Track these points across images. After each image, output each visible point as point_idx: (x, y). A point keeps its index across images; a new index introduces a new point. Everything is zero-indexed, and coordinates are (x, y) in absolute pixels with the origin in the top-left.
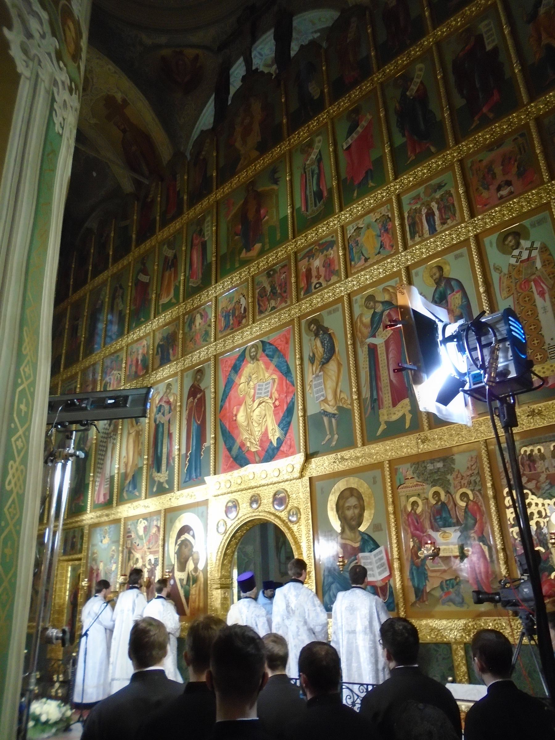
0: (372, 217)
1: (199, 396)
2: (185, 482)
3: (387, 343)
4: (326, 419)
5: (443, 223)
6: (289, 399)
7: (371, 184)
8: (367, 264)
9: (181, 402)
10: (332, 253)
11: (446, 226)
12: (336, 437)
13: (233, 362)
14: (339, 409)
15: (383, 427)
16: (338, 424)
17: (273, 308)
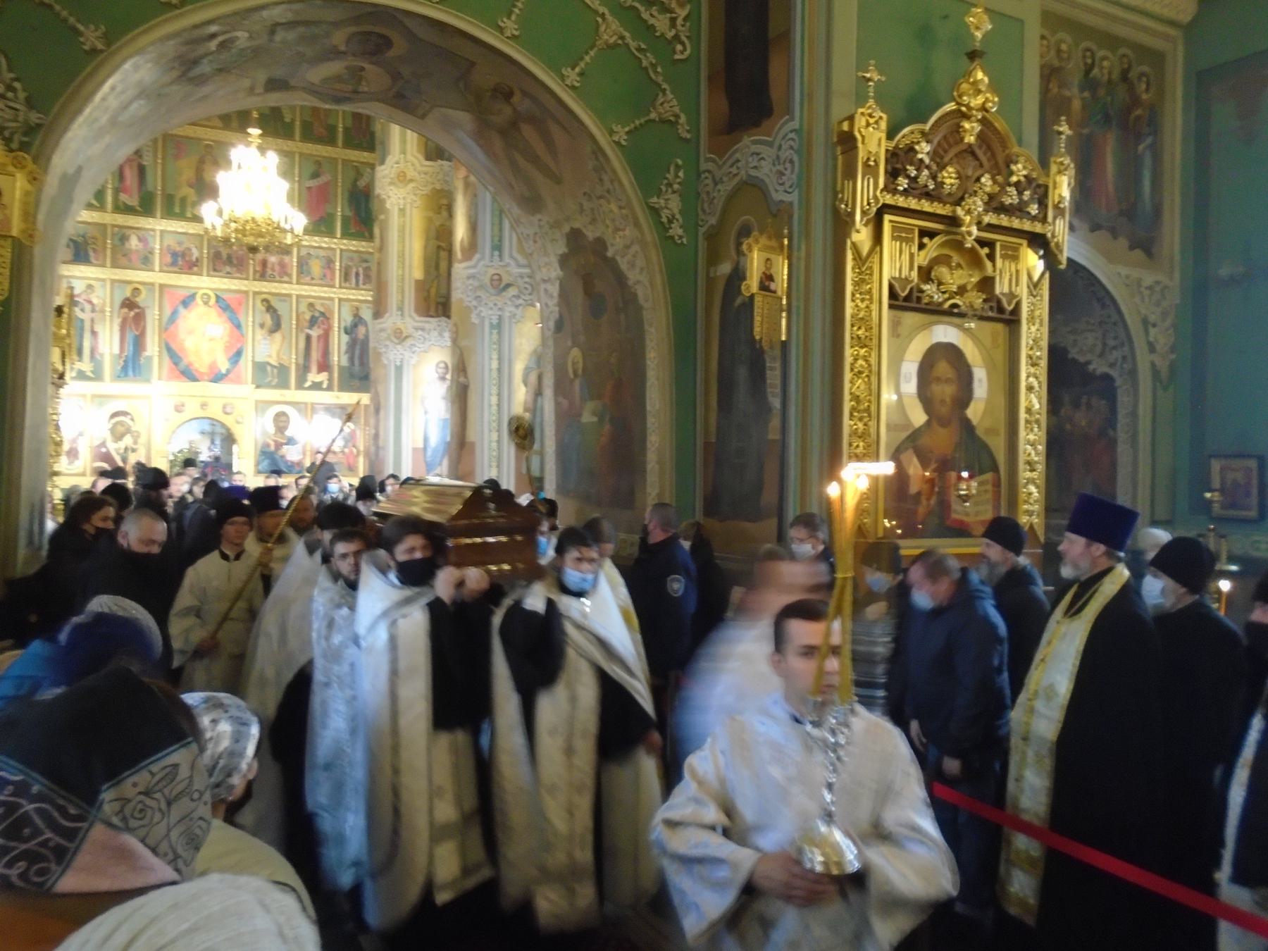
0: (322, 253)
1: (137, 310)
2: (119, 377)
3: (319, 337)
4: (269, 368)
5: (364, 284)
6: (239, 346)
7: (323, 229)
8: (314, 282)
9: (112, 306)
10: (286, 259)
11: (364, 287)
12: (276, 380)
13: (182, 299)
14: (280, 364)
15: (308, 384)
16: (279, 373)
17: (228, 273)
